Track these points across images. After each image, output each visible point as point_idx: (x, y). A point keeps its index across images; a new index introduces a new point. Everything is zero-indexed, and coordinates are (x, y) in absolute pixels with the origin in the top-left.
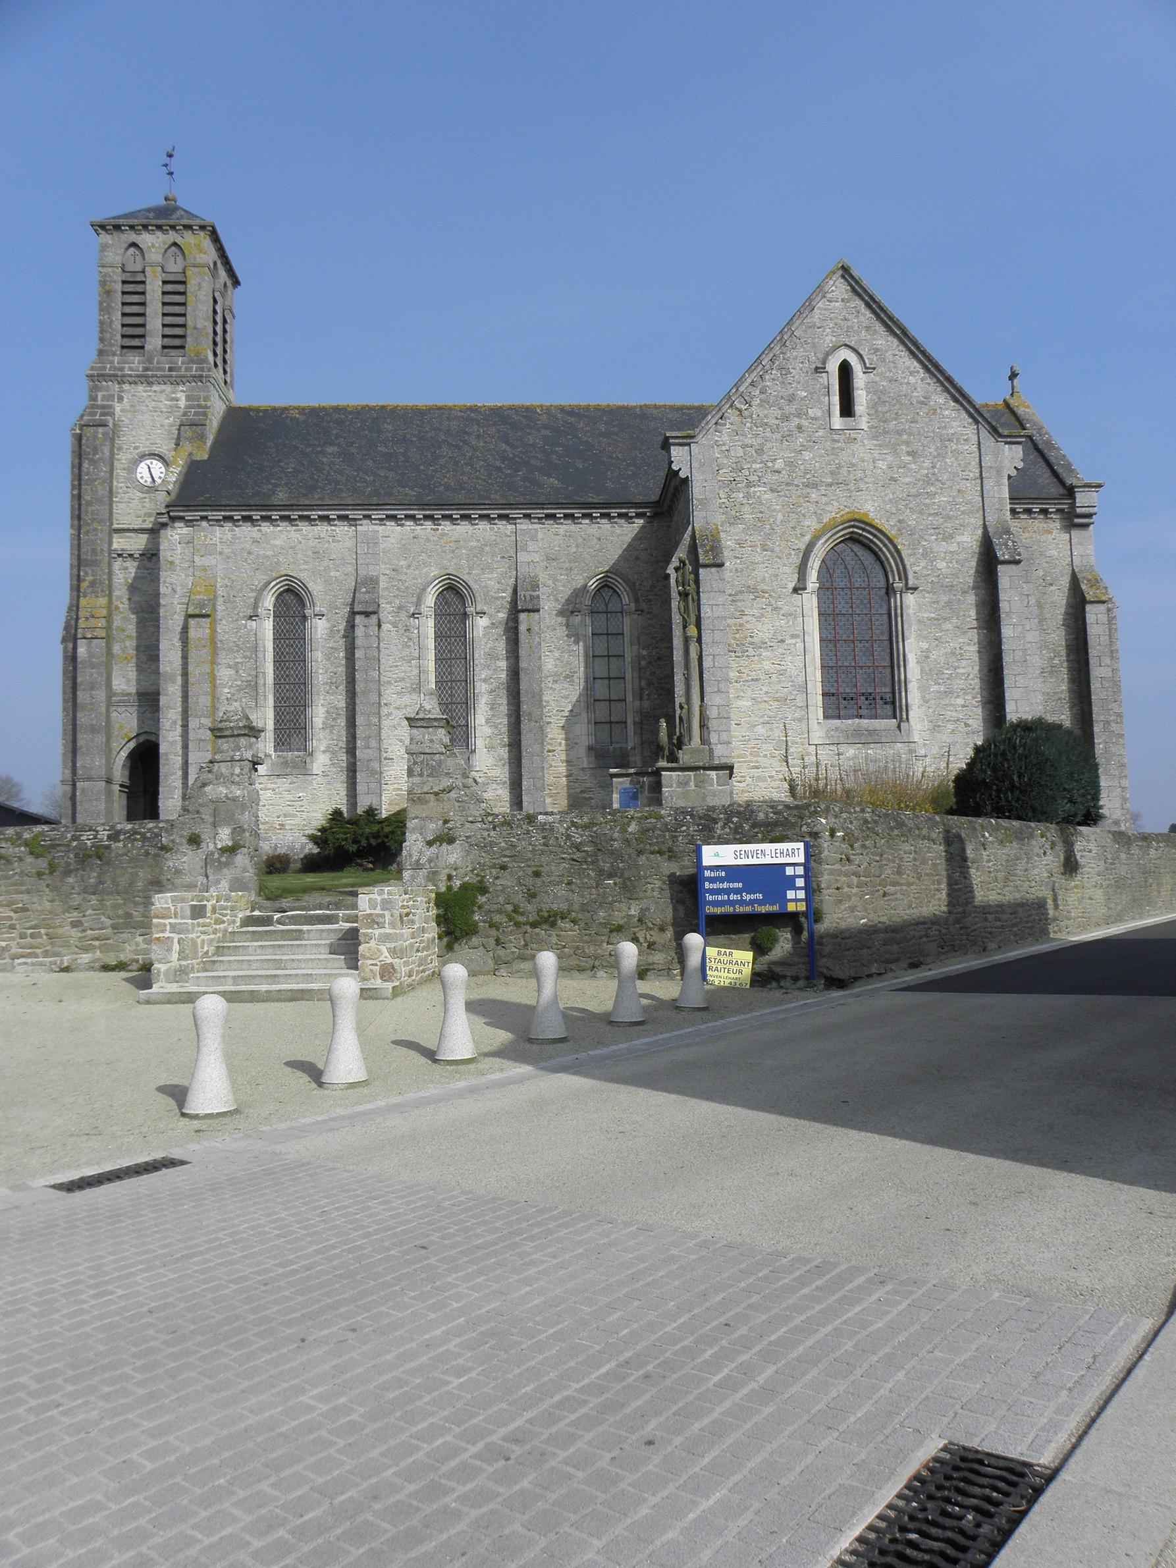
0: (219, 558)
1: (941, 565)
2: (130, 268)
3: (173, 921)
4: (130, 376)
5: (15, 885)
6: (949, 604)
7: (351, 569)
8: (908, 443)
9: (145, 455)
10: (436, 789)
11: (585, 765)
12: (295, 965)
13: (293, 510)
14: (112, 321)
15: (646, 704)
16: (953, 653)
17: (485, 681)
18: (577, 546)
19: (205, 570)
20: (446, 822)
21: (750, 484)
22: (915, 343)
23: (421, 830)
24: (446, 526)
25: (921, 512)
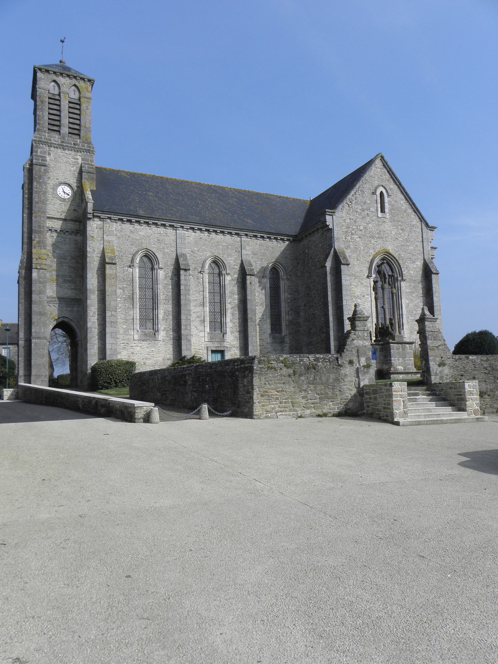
0: (115, 237)
1: (412, 272)
2: (51, 92)
3: (400, 393)
4: (55, 144)
5: (278, 380)
6: (414, 287)
7: (174, 249)
8: (401, 226)
9: (61, 183)
10: (437, 345)
11: (269, 341)
12: (435, 410)
13: (150, 220)
14: (43, 116)
15: (290, 318)
16: (416, 305)
17: (230, 303)
18: (264, 250)
19: (109, 242)
20: (442, 358)
21: (352, 234)
22: (404, 189)
23: (434, 360)
24: (213, 235)
25: (405, 252)
